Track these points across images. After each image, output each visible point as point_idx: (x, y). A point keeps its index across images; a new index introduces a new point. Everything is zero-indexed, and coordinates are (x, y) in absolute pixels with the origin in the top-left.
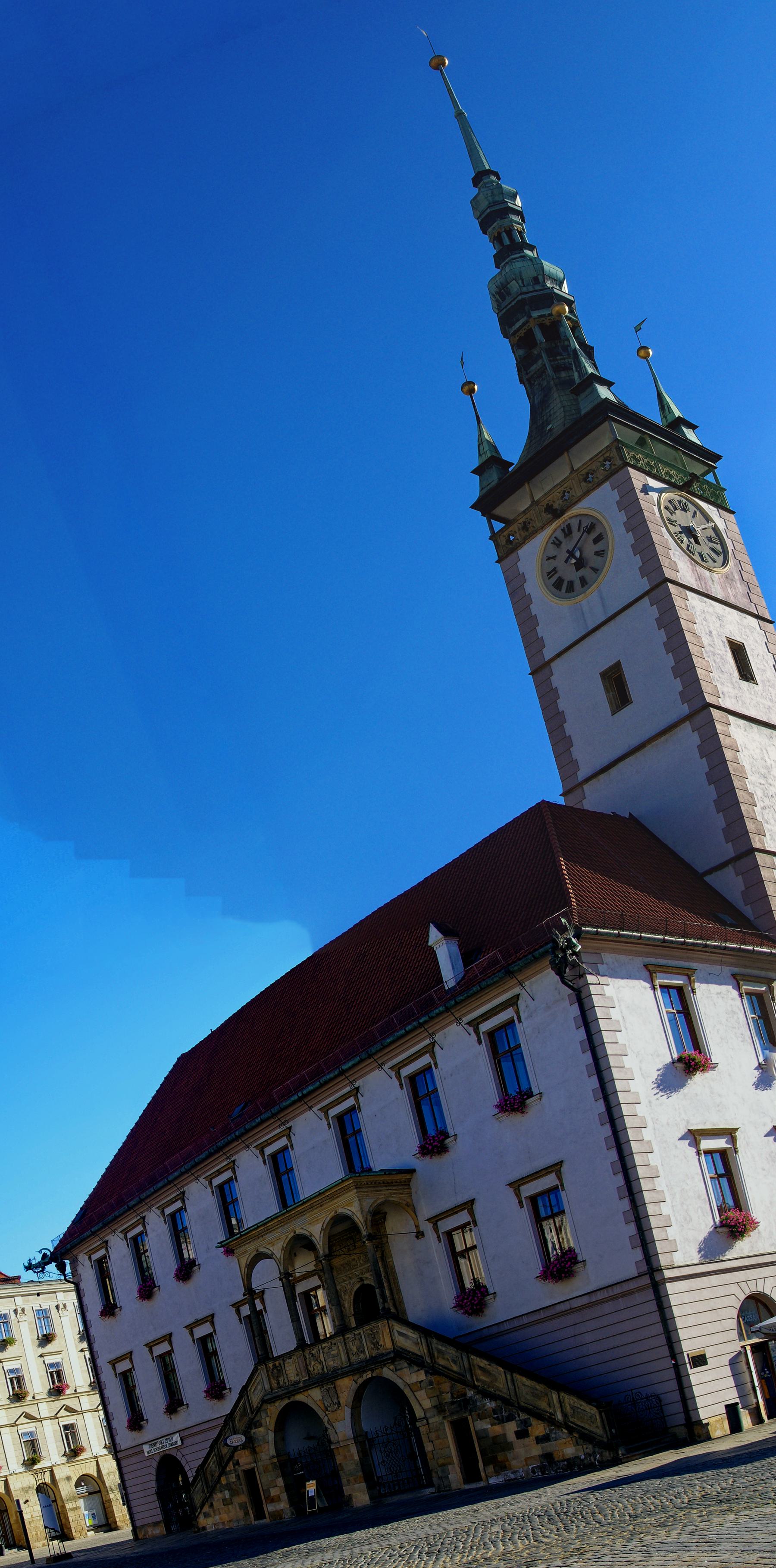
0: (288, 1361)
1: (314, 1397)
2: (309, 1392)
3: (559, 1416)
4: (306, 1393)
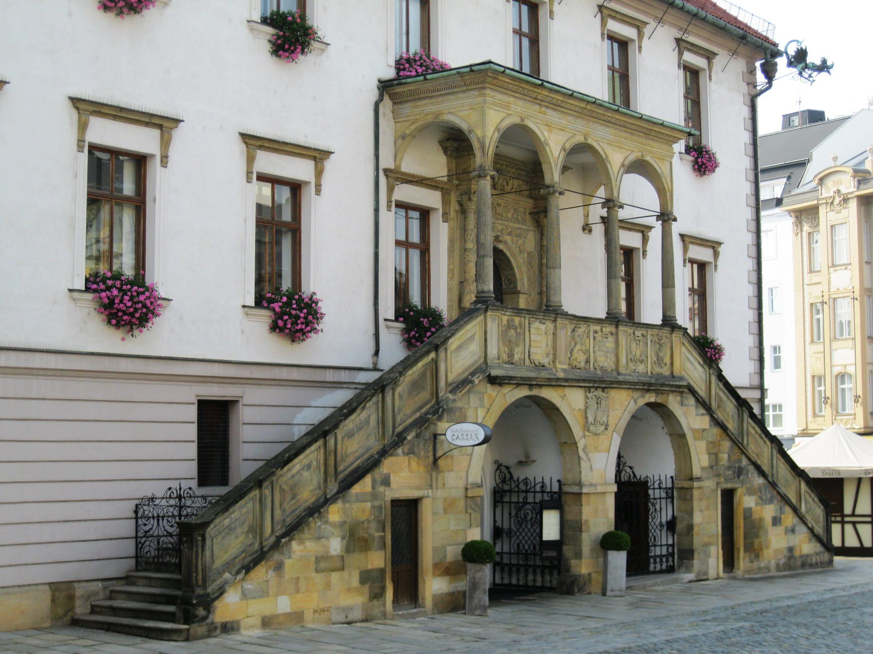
0: (536, 325)
1: (571, 402)
2: (568, 391)
3: (803, 509)
4: (560, 391)
